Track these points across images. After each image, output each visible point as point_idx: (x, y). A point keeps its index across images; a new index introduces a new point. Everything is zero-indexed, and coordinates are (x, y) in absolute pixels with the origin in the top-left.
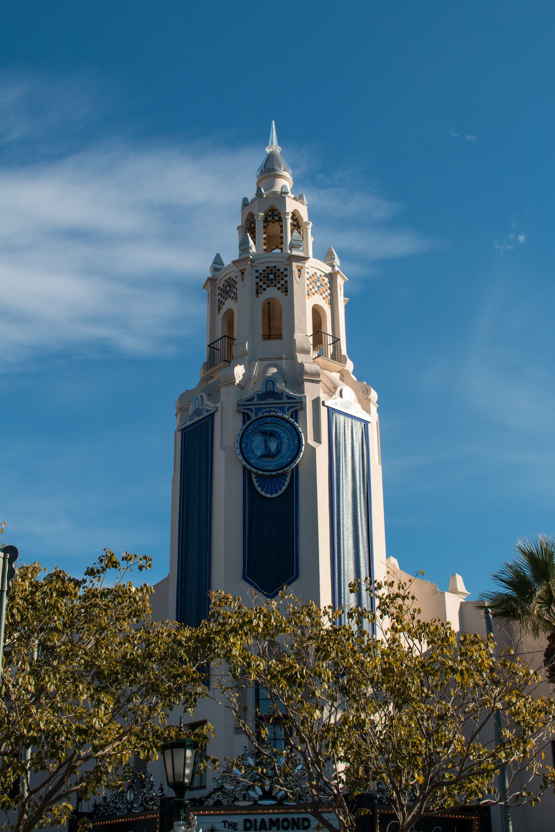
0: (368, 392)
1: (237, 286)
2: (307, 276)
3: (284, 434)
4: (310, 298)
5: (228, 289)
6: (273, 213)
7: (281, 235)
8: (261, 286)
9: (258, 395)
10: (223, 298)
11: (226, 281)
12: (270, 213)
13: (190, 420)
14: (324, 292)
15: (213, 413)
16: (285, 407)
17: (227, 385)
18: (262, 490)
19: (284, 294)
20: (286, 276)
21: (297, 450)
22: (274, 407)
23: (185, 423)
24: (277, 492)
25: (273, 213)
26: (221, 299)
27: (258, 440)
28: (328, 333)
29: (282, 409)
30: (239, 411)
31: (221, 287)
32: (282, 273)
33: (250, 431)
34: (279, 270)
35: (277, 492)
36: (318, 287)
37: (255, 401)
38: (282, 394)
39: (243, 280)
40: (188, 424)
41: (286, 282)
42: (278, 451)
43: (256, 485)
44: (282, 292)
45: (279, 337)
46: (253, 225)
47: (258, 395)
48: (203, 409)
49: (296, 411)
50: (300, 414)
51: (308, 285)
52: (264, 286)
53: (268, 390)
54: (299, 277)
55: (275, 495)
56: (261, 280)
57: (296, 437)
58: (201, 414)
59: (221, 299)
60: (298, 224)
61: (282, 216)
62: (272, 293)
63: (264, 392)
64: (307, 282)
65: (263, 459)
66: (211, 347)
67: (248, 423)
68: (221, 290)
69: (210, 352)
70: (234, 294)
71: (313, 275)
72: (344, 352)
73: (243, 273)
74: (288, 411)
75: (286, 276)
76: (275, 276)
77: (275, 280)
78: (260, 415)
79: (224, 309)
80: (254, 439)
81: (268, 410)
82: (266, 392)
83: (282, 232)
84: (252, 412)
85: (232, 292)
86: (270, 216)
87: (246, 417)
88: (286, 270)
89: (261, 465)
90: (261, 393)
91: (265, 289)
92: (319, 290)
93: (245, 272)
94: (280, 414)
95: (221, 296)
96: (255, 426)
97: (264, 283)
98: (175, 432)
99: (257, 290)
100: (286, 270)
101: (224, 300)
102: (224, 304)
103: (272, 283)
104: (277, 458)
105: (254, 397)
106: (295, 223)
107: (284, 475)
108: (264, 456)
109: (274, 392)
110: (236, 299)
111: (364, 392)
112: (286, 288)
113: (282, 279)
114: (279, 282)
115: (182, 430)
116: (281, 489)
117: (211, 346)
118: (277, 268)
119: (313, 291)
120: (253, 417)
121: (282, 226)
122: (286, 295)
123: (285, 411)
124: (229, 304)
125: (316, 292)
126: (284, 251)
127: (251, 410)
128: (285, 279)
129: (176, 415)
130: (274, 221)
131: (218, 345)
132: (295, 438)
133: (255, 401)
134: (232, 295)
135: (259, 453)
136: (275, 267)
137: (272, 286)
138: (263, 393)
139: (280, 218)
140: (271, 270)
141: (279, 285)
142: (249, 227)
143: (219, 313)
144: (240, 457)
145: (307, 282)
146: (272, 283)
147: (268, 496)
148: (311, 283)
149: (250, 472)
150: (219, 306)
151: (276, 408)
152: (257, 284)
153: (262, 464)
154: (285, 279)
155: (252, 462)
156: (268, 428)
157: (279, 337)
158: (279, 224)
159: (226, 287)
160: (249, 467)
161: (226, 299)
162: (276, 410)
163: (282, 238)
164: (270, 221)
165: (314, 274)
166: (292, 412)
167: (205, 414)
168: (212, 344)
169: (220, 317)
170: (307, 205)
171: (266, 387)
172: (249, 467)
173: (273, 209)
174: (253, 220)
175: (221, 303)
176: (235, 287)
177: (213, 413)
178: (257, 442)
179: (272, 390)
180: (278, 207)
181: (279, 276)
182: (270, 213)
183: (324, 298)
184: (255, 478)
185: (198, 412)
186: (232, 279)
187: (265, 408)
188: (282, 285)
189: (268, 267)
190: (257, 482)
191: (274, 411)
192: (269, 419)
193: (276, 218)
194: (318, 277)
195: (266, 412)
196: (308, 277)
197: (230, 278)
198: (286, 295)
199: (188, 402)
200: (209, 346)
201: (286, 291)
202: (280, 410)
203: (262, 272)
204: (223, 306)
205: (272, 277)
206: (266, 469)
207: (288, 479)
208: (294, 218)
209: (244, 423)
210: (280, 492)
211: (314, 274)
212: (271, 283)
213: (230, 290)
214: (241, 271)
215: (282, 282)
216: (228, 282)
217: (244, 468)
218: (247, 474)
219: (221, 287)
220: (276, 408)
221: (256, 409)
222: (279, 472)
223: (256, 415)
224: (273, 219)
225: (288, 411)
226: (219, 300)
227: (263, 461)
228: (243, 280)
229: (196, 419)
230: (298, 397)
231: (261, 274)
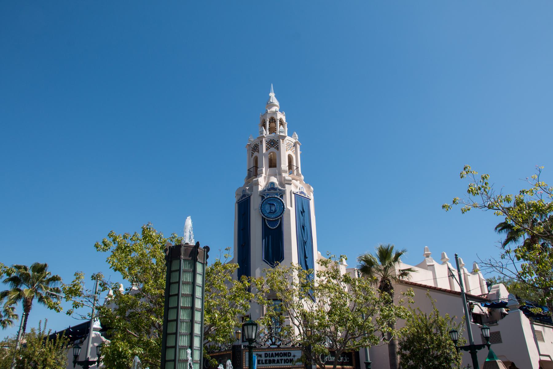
0: (309, 188)
2: (286, 143)
6: (272, 119)
7: (276, 127)
8: (268, 147)
9: (268, 189)
12: (271, 119)
13: (241, 199)
15: (250, 196)
16: (277, 194)
17: (256, 185)
18: (269, 226)
19: (277, 150)
23: (239, 200)
24: (275, 227)
25: (272, 119)
26: (253, 152)
29: (277, 194)
30: (260, 195)
31: (253, 147)
32: (276, 142)
34: (275, 141)
35: (275, 227)
36: (290, 147)
37: (267, 191)
38: (277, 189)
40: (240, 200)
41: (278, 145)
42: (275, 211)
43: (267, 224)
46: (264, 124)
47: (268, 189)
50: (284, 196)
51: (286, 147)
55: (274, 228)
56: (268, 145)
58: (246, 196)
59: (253, 152)
61: (276, 120)
62: (272, 149)
63: (270, 187)
64: (286, 146)
65: (270, 214)
67: (264, 200)
71: (288, 143)
72: (300, 172)
73: (261, 142)
75: (278, 143)
76: (273, 143)
77: (274, 144)
78: (268, 197)
79: (254, 156)
80: (266, 206)
82: (271, 188)
83: (276, 126)
86: (271, 120)
87: (263, 197)
88: (278, 141)
91: (270, 148)
94: (276, 196)
97: (269, 146)
98: (235, 203)
99: (267, 148)
101: (254, 153)
102: (254, 154)
103: (272, 146)
104: (275, 213)
106: (281, 123)
107: (278, 220)
108: (270, 212)
109: (274, 188)
112: (278, 148)
113: (276, 144)
114: (275, 146)
115: (238, 203)
116: (277, 225)
117: (250, 170)
119: (288, 149)
120: (266, 198)
121: (276, 124)
122: (278, 150)
124: (256, 154)
125: (289, 149)
126: (277, 133)
127: (264, 194)
128: (278, 144)
129: (236, 197)
131: (252, 170)
133: (267, 191)
134: (257, 150)
135: (268, 211)
136: (273, 140)
137: (272, 147)
139: (275, 121)
140: (272, 141)
141: (275, 147)
144: (261, 213)
145: (286, 146)
146: (272, 146)
147: (272, 228)
149: (265, 219)
150: (252, 155)
151: (275, 194)
152: (267, 146)
153: (269, 216)
154: (278, 144)
155: (265, 215)
156: (271, 202)
157: (275, 166)
160: (264, 217)
162: (275, 195)
163: (276, 128)
166: (281, 196)
167: (247, 196)
169: (252, 159)
170: (285, 116)
171: (271, 186)
172: (264, 217)
177: (250, 196)
178: (267, 206)
180: (274, 116)
182: (271, 119)
183: (292, 152)
185: (244, 196)
187: (270, 194)
188: (276, 147)
189: (271, 140)
190: (267, 222)
191: (274, 195)
192: (272, 198)
193: (274, 121)
195: (271, 195)
201: (278, 149)
204: (254, 155)
205: (272, 143)
206: (271, 217)
207: (279, 221)
209: (262, 200)
210: (276, 227)
214: (260, 141)
215: (276, 145)
217: (262, 217)
218: (263, 220)
219: (253, 147)
220: (275, 194)
222: (276, 219)
223: (267, 196)
224: (272, 121)
229: (244, 198)
231: (268, 142)
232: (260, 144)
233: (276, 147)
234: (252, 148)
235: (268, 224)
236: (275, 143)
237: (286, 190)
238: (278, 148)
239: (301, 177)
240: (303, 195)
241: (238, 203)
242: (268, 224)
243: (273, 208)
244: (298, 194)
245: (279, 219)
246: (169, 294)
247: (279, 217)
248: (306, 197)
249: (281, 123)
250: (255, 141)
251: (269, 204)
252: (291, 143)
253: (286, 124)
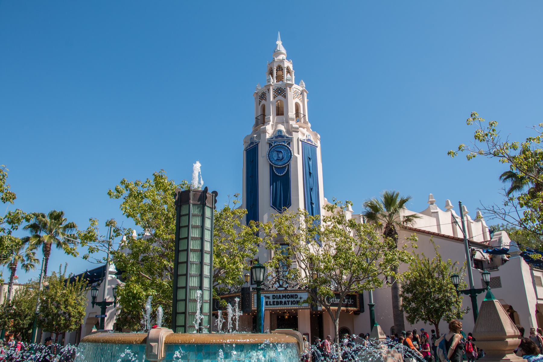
0: (316, 135)
5: (263, 96)
8: (275, 95)
15: (258, 144)
17: (263, 133)
18: (277, 173)
20: (285, 91)
24: (282, 173)
29: (284, 142)
30: (268, 143)
34: (282, 89)
37: (274, 139)
40: (248, 148)
41: (285, 93)
42: (283, 158)
43: (275, 171)
49: (290, 143)
50: (291, 143)
52: (277, 95)
55: (282, 175)
56: (275, 93)
58: (253, 144)
61: (283, 68)
62: (280, 97)
63: (277, 135)
65: (277, 161)
67: (271, 147)
72: (307, 120)
73: (268, 90)
75: (285, 91)
78: (276, 144)
79: (261, 104)
83: (283, 74)
87: (270, 145)
88: (285, 89)
91: (277, 96)
94: (283, 144)
97: (277, 94)
99: (274, 96)
100: (285, 89)
104: (282, 160)
107: (285, 167)
108: (278, 160)
113: (284, 92)
115: (246, 150)
116: (284, 172)
119: (295, 97)
120: (273, 145)
121: (283, 72)
122: (285, 98)
124: (263, 102)
128: (285, 92)
131: (259, 118)
133: (274, 139)
135: (275, 159)
139: (282, 69)
141: (282, 95)
147: (279, 175)
149: (272, 166)
152: (274, 94)
153: (276, 163)
154: (285, 92)
156: (279, 149)
157: (282, 114)
167: (255, 144)
178: (275, 155)
180: (281, 64)
185: (252, 143)
188: (284, 95)
189: (278, 88)
198: (285, 98)
201: (285, 97)
205: (279, 91)
207: (287, 168)
209: (270, 147)
210: (284, 173)
212: (279, 94)
215: (284, 94)
217: (270, 164)
218: (271, 166)
229: (252, 146)
231: (275, 90)
232: (267, 93)
238: (285, 96)
239: (308, 124)
240: (309, 142)
243: (281, 156)
244: (305, 141)
248: (313, 144)
249: (288, 71)
250: (263, 89)
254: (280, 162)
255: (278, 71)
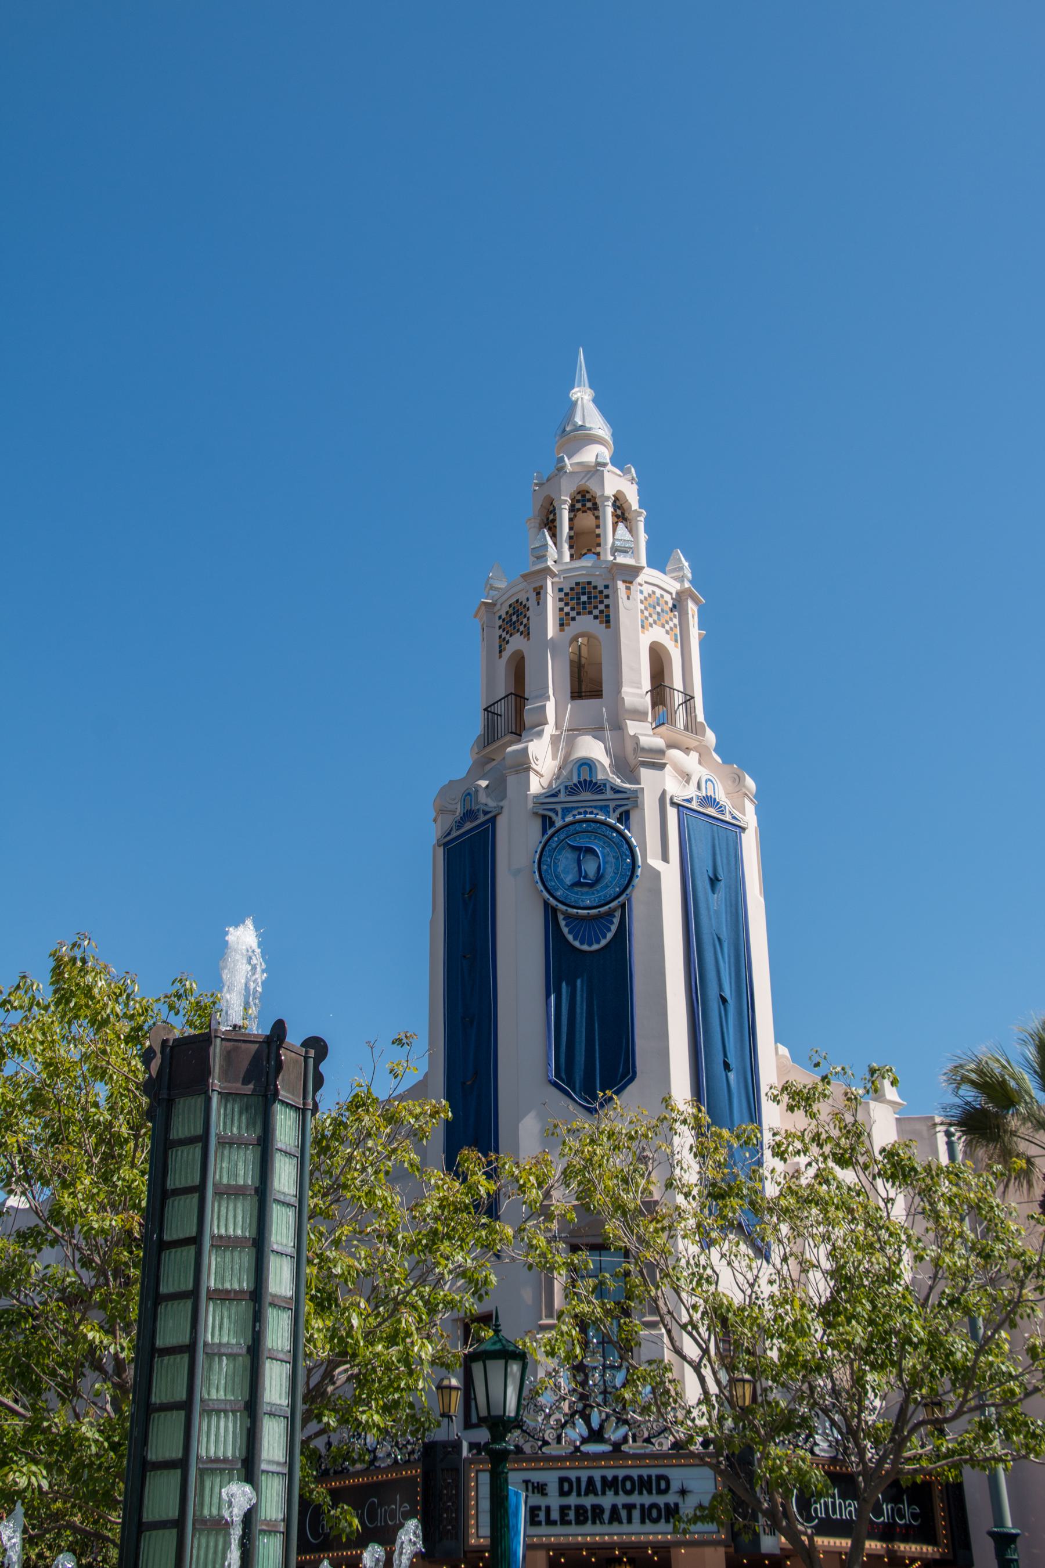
0: (739, 780)
1: (528, 614)
2: (641, 597)
3: (608, 849)
4: (646, 632)
5: (514, 618)
6: (583, 496)
7: (598, 531)
8: (567, 614)
9: (566, 787)
10: (507, 633)
11: (510, 606)
12: (579, 497)
13: (459, 827)
14: (667, 623)
16: (608, 806)
17: (517, 772)
18: (575, 938)
20: (607, 597)
21: (629, 874)
22: (591, 807)
23: (449, 834)
24: (598, 942)
25: (583, 496)
26: (504, 635)
27: (567, 858)
28: (675, 687)
29: (605, 809)
30: (536, 814)
32: (601, 592)
33: (554, 845)
34: (595, 588)
35: (598, 942)
36: (658, 614)
38: (605, 785)
39: (538, 604)
40: (454, 834)
41: (607, 606)
42: (599, 877)
43: (565, 930)
44: (601, 622)
45: (596, 693)
46: (551, 517)
48: (478, 810)
49: (627, 813)
50: (634, 817)
51: (642, 612)
53: (582, 780)
54: (628, 598)
55: (595, 947)
56: (567, 604)
57: (628, 853)
58: (476, 818)
59: (504, 635)
60: (623, 514)
61: (598, 501)
62: (586, 623)
63: (575, 780)
64: (642, 607)
65: (576, 889)
66: (488, 711)
67: (550, 832)
68: (504, 620)
69: (488, 719)
70: (525, 626)
71: (649, 595)
72: (701, 717)
73: (538, 594)
74: (614, 811)
75: (607, 597)
76: (589, 598)
77: (590, 603)
78: (569, 819)
79: (509, 650)
80: (560, 857)
81: (582, 810)
82: (580, 782)
83: (598, 527)
84: (557, 815)
85: (522, 623)
86: (578, 501)
87: (547, 822)
88: (607, 587)
89: (573, 899)
90: (571, 784)
91: (573, 619)
92: (659, 619)
93: (542, 591)
95: (504, 630)
96: (562, 837)
97: (573, 609)
98: (434, 846)
99: (561, 619)
100: (607, 587)
102: (508, 642)
104: (598, 887)
105: (559, 791)
106: (619, 512)
107: (610, 914)
108: (578, 884)
109: (591, 781)
110: (529, 634)
111: (734, 781)
112: (608, 616)
113: (601, 602)
114: (596, 607)
115: (445, 845)
116: (605, 937)
118: (593, 584)
119: (651, 620)
120: (559, 823)
121: (597, 518)
122: (608, 627)
123: (609, 812)
124: (516, 642)
125: (655, 622)
126: (602, 557)
128: (606, 602)
129: (435, 820)
130: (585, 509)
131: (500, 708)
132: (626, 855)
133: (562, 797)
134: (522, 628)
135: (569, 879)
136: (589, 583)
138: (575, 785)
139: (595, 504)
141: (596, 612)
142: (545, 520)
143: (500, 657)
144: (540, 887)
145: (642, 607)
146: (584, 608)
147: (585, 947)
148: (646, 609)
149: (555, 910)
150: (500, 646)
151: (595, 807)
152: (561, 610)
153: (573, 898)
154: (606, 602)
155: (558, 893)
157: (596, 693)
158: (594, 515)
159: (511, 616)
160: (552, 901)
161: (511, 635)
162: (595, 811)
163: (598, 536)
164: (579, 510)
165: (651, 592)
166: (621, 814)
167: (482, 818)
168: (490, 706)
169: (502, 664)
170: (637, 484)
171: (579, 775)
172: (552, 901)
173: (583, 491)
174: (551, 508)
175: (503, 642)
176: (525, 616)
178: (565, 861)
179: (588, 779)
180: (592, 486)
181: (596, 597)
182: (579, 497)
183: (667, 632)
184: (564, 919)
185: (469, 815)
186: (521, 603)
187: (578, 808)
188: (601, 612)
189: (578, 584)
190: (567, 925)
191: (591, 813)
194: (658, 598)
195: (580, 814)
196: (643, 599)
197: (517, 601)
198: (608, 627)
199: (454, 800)
200: (485, 710)
201: (608, 622)
202: (601, 810)
203: (568, 591)
204: (508, 647)
205: (584, 598)
206: (582, 904)
207: (616, 921)
208: (618, 504)
209: (544, 832)
210: (603, 942)
211: (651, 592)
212: (583, 608)
213: (518, 621)
214: (535, 589)
215: (601, 607)
216: (514, 608)
217: (546, 904)
218: (550, 913)
220: (595, 807)
221: (563, 809)
222: (602, 909)
223: (563, 818)
224: (584, 505)
225: (614, 811)
226: (500, 637)
227: (577, 893)
228: (538, 604)
229: (468, 826)
230: (629, 789)
231: (566, 594)
232: (532, 604)
233: (601, 612)
234: (500, 617)
235: (570, 932)
236: (596, 597)
237: (643, 788)
238: (607, 618)
239: (703, 734)
240: (711, 811)
241: (445, 845)
242: (570, 932)
243: (590, 867)
244: (694, 805)
245: (615, 910)
246: (153, 1344)
247: (612, 905)
248: (728, 818)
249: (619, 512)
251: (574, 848)
252: (662, 596)
253: (642, 519)
254: (587, 893)
255: (580, 514)
